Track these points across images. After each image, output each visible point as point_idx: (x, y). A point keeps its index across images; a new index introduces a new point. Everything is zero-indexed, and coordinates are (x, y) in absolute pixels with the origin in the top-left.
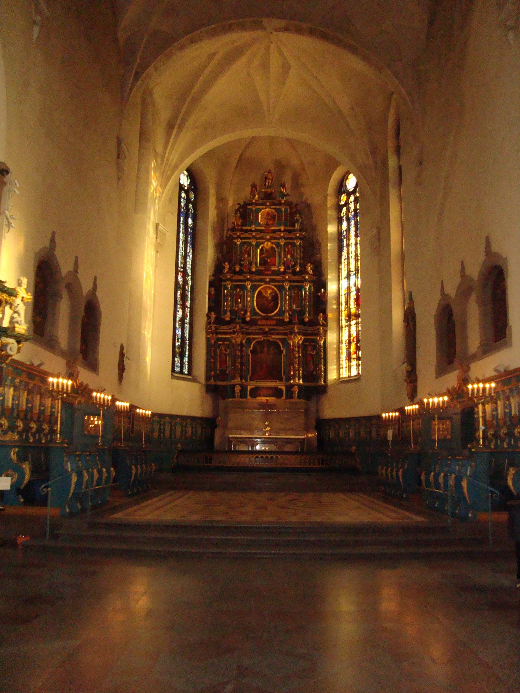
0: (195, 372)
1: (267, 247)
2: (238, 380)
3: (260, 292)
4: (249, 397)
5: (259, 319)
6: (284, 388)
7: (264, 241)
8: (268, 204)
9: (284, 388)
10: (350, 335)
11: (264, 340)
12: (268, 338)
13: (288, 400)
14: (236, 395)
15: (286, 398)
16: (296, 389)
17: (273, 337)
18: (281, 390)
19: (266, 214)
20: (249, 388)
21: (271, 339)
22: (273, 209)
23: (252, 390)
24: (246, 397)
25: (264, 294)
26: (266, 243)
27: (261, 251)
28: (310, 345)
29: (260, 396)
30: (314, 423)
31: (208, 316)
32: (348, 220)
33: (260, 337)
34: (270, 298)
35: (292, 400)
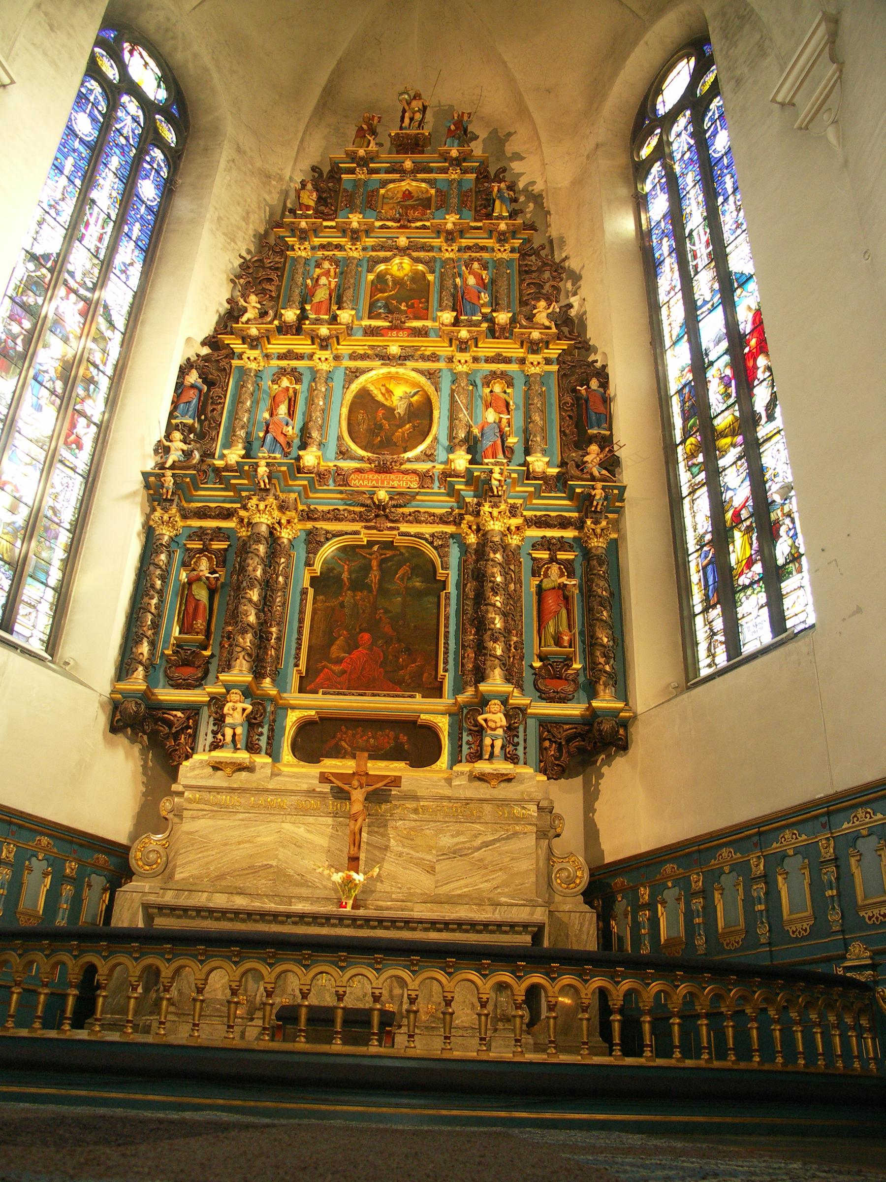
0: (72, 647)
1: (401, 274)
2: (240, 673)
3: (364, 395)
4: (287, 755)
5: (359, 471)
6: (443, 723)
7: (389, 254)
8: (408, 165)
9: (443, 723)
10: (718, 506)
11: (371, 544)
12: (386, 536)
13: (464, 767)
14: (229, 732)
16: (496, 717)
17: (404, 528)
18: (431, 731)
19: (400, 195)
20: (292, 718)
21: (399, 541)
22: (423, 181)
23: (305, 727)
24: (273, 753)
25: (380, 398)
26: (397, 260)
27: (381, 277)
28: (553, 559)
29: (337, 753)
30: (583, 878)
31: (162, 449)
32: (672, 185)
33: (357, 526)
34: (401, 410)
35: (483, 766)
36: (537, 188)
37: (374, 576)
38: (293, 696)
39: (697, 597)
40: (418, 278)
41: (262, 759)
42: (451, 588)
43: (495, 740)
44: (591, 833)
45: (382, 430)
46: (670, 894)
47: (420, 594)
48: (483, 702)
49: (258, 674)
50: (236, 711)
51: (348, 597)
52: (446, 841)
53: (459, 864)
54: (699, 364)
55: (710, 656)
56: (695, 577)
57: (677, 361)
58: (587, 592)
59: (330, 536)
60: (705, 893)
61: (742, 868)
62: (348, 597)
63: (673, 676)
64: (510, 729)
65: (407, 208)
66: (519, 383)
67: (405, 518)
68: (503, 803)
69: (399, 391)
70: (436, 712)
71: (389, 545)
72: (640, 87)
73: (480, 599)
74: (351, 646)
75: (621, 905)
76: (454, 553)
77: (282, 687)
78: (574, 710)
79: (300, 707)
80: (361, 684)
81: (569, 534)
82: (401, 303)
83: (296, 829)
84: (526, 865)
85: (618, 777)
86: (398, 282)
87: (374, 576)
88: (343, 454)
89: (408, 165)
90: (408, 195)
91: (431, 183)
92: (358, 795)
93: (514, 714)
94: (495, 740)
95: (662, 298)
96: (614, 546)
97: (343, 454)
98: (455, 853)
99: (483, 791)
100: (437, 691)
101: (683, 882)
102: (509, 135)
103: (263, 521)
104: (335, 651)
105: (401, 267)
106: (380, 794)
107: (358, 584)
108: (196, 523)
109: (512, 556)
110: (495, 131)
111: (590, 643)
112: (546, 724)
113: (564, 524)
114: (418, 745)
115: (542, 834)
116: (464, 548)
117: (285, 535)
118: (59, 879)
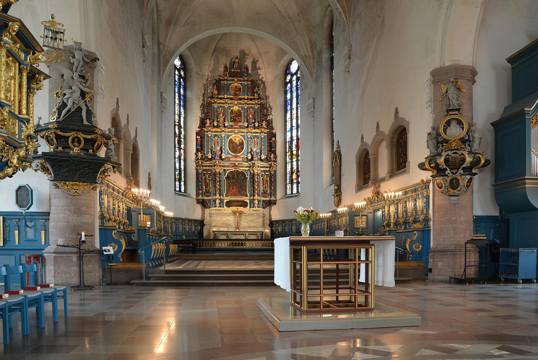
3: (231, 140)
6: (248, 201)
9: (248, 201)
13: (252, 209)
15: (250, 207)
16: (256, 202)
17: (240, 168)
20: (225, 201)
23: (227, 202)
24: (223, 207)
33: (232, 168)
34: (238, 143)
35: (254, 209)
36: (264, 80)
37: (236, 176)
38: (225, 197)
39: (288, 181)
40: (239, 111)
41: (222, 208)
42: (248, 179)
43: (256, 205)
44: (270, 215)
45: (236, 148)
46: (280, 226)
47: (243, 180)
48: (254, 200)
49: (220, 196)
50: (218, 202)
51: (231, 180)
52: (250, 219)
53: (251, 222)
54: (292, 137)
55: (289, 192)
56: (288, 178)
57: (289, 135)
58: (270, 180)
59: (228, 170)
60: (285, 227)
61: (289, 224)
62: (231, 180)
63: (283, 194)
64: (258, 203)
65: (236, 91)
66: (260, 138)
67: (240, 167)
68: (257, 214)
69: (237, 139)
70: (247, 199)
71: (238, 171)
72: (287, 62)
73: (254, 183)
74: (233, 189)
75: (274, 226)
76: (249, 173)
77: (223, 197)
78: (268, 199)
79: (226, 199)
80: (235, 195)
81: (268, 169)
82: (236, 117)
83: (228, 218)
84: (261, 222)
85: (274, 207)
86: (235, 112)
87: (236, 176)
88: (228, 154)
89: (236, 80)
90: (236, 87)
91: (241, 84)
92: (238, 214)
93: (259, 201)
94: (256, 205)
95: (287, 120)
96: (275, 171)
97: (228, 154)
98: (251, 221)
99: (255, 212)
100: (247, 196)
101: (282, 225)
102: (258, 61)
103: (218, 170)
104: (230, 190)
105: (236, 108)
106: (241, 213)
107: (233, 178)
108: (204, 168)
109: (258, 175)
110: (254, 59)
111: (271, 188)
112: (263, 201)
113: (267, 167)
114: (244, 204)
115: (263, 217)
116: (251, 173)
117: (221, 172)
118: (195, 226)
